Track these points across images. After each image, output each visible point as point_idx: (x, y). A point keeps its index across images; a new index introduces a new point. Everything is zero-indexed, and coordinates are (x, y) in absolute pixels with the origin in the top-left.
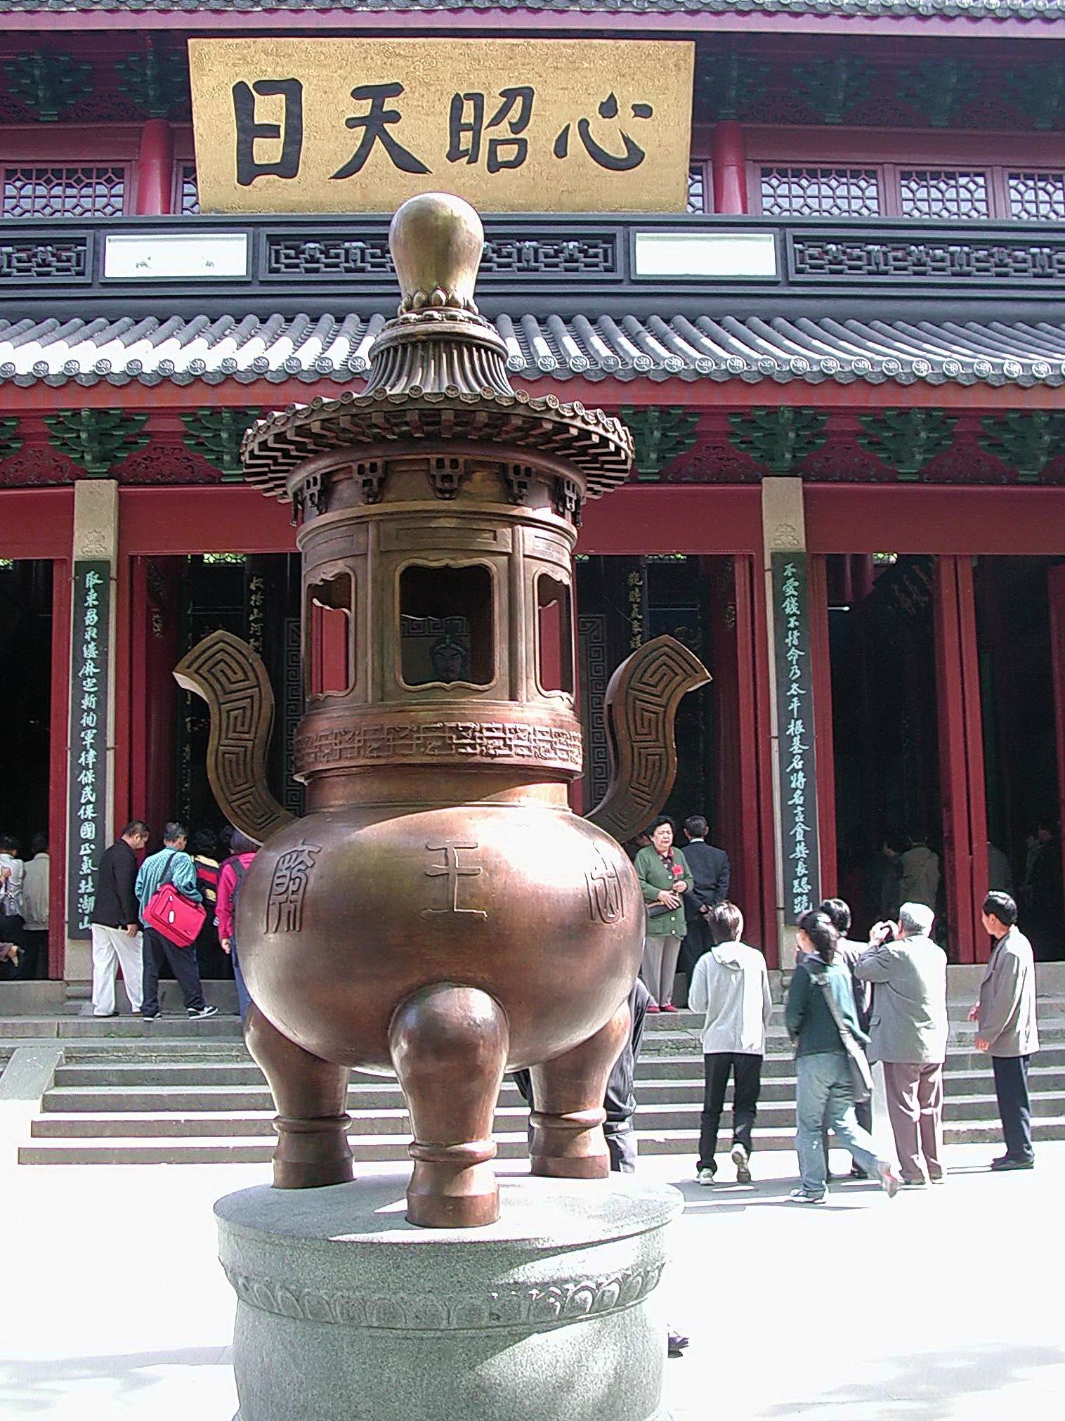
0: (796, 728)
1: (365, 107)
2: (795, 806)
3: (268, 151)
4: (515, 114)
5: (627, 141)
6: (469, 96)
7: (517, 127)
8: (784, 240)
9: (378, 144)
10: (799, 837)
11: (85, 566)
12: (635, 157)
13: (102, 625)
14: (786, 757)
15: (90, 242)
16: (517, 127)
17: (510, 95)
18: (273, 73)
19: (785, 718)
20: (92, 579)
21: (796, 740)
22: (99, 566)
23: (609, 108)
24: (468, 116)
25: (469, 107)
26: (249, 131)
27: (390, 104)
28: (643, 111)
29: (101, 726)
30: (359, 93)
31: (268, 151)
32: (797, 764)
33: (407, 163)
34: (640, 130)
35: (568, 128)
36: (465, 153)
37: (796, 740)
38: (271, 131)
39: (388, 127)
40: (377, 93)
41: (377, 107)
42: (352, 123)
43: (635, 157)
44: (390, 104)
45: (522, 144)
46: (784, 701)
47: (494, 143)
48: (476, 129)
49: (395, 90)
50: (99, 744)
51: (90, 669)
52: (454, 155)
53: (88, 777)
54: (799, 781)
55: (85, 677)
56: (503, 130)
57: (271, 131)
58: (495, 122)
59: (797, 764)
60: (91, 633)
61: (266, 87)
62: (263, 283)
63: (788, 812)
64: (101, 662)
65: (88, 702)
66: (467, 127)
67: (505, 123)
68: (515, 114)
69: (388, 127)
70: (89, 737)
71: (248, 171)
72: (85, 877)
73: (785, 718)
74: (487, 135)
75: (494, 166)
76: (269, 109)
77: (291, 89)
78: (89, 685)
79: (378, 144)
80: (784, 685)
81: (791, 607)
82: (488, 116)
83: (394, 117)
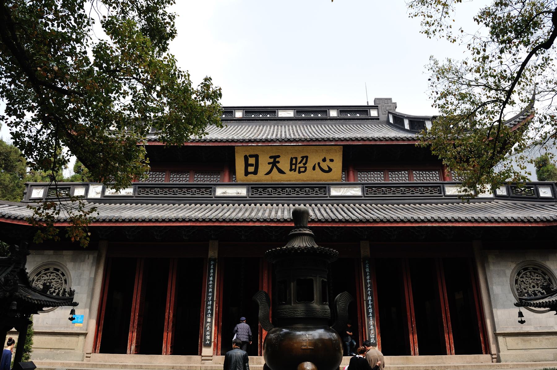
0: (370, 298)
1: (272, 160)
2: (370, 317)
3: (251, 169)
4: (304, 161)
5: (328, 167)
6: (294, 158)
7: (304, 164)
8: (363, 187)
9: (275, 169)
10: (371, 324)
11: (211, 259)
12: (330, 170)
13: (214, 273)
14: (368, 305)
15: (213, 188)
16: (304, 164)
17: (303, 158)
18: (252, 153)
20: (212, 263)
21: (370, 301)
22: (214, 260)
23: (324, 160)
24: (294, 162)
25: (294, 160)
26: (247, 165)
27: (277, 160)
28: (332, 160)
29: (213, 296)
30: (271, 157)
31: (251, 169)
32: (370, 306)
33: (281, 171)
34: (331, 165)
35: (315, 164)
36: (293, 169)
37: (370, 301)
38: (252, 165)
39: (277, 164)
40: (275, 157)
41: (275, 160)
42: (269, 163)
43: (330, 170)
44: (277, 160)
45: (306, 168)
46: (367, 291)
47: (300, 168)
48: (296, 164)
49: (279, 156)
50: (212, 300)
51: (211, 282)
52: (291, 170)
53: (209, 307)
54: (371, 311)
55: (210, 284)
56: (301, 165)
57: (252, 165)
58: (300, 163)
59: (370, 306)
60: (212, 274)
61: (251, 156)
62: (250, 197)
64: (213, 281)
65: (210, 290)
66: (294, 164)
67: (302, 163)
68: (304, 161)
69: (277, 164)
70: (210, 298)
71: (247, 173)
72: (208, 331)
73: (367, 295)
74: (298, 166)
75: (300, 172)
77: (256, 157)
78: (211, 286)
79: (275, 169)
80: (366, 288)
81: (367, 270)
82: (298, 162)
83: (278, 162)
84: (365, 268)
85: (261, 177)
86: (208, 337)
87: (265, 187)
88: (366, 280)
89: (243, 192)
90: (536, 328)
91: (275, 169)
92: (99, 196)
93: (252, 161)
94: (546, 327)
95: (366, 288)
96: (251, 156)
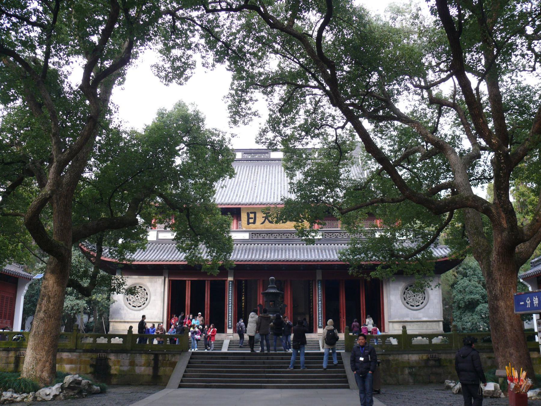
0: (320, 302)
1: (265, 215)
3: (251, 221)
14: (319, 306)
19: (319, 301)
26: (249, 218)
31: (251, 221)
38: (252, 218)
46: (318, 299)
50: (232, 303)
54: (320, 309)
57: (252, 218)
63: (319, 313)
71: (249, 223)
73: (319, 301)
76: (252, 216)
79: (267, 221)
80: (318, 297)
81: (320, 287)
84: (318, 286)
85: (258, 226)
86: (230, 324)
87: (259, 233)
88: (318, 292)
89: (246, 236)
90: (411, 319)
91: (267, 221)
92: (155, 239)
93: (252, 216)
94: (417, 318)
95: (318, 297)
96: (251, 213)
